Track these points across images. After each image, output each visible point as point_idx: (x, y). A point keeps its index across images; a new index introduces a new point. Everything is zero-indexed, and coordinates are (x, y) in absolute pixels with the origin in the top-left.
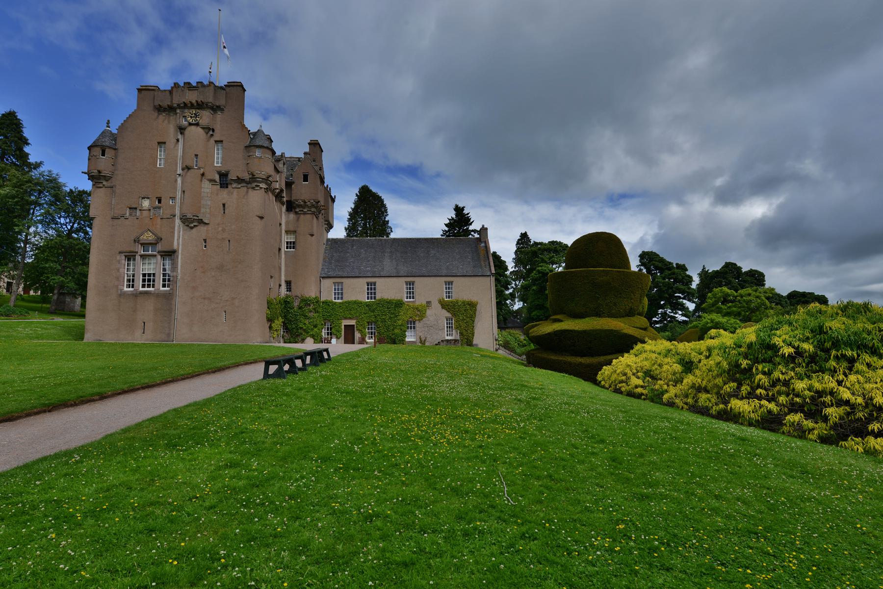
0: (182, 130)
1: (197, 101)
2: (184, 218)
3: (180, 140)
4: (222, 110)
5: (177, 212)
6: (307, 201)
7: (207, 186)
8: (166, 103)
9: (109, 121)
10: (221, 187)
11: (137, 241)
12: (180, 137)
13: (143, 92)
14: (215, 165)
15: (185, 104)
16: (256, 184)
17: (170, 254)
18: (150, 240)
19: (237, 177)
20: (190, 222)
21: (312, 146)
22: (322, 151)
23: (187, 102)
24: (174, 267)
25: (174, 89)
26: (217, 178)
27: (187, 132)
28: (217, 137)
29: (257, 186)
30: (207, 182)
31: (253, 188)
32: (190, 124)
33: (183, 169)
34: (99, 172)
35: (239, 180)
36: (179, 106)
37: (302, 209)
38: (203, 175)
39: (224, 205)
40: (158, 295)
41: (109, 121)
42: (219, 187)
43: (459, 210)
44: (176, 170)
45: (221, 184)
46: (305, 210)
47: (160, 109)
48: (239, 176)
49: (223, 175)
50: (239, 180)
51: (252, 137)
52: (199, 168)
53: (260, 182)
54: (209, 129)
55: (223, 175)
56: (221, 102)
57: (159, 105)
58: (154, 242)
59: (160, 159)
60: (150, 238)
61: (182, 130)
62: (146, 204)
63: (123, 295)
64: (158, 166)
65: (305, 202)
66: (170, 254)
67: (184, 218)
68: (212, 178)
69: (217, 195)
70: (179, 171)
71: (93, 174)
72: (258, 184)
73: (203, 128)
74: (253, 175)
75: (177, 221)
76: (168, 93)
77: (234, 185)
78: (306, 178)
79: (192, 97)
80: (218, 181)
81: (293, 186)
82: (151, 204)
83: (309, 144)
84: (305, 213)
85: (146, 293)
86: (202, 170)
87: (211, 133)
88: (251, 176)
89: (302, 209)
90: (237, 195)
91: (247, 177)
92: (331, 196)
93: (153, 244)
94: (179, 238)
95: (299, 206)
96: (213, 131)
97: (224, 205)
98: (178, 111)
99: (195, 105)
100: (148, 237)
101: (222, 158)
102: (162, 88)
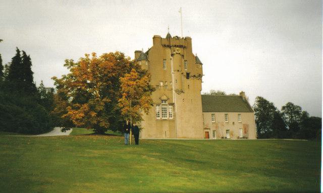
5: (173, 88)
8: (167, 43)
17: (173, 104)
20: (180, 92)
24: (174, 109)
33: (174, 71)
36: (173, 46)
40: (170, 121)
47: (165, 46)
63: (157, 120)
66: (173, 104)
70: (172, 71)
75: (174, 92)
77: (192, 78)
79: (178, 43)
85: (165, 120)
94: (175, 98)
98: (172, 48)
100: (164, 98)
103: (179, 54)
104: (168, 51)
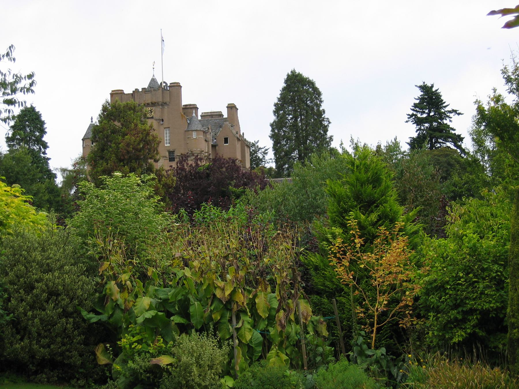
4: (168, 105)
9: (92, 117)
10: (170, 161)
13: (114, 95)
14: (166, 145)
21: (230, 109)
22: (237, 109)
25: (136, 94)
26: (167, 154)
41: (92, 117)
43: (426, 89)
45: (169, 158)
54: (160, 120)
56: (167, 100)
68: (164, 155)
73: (156, 120)
76: (131, 96)
78: (226, 140)
79: (148, 99)
80: (168, 157)
81: (217, 148)
83: (227, 107)
96: (163, 120)
99: (150, 104)
101: (169, 140)
102: (126, 92)
103: (152, 118)
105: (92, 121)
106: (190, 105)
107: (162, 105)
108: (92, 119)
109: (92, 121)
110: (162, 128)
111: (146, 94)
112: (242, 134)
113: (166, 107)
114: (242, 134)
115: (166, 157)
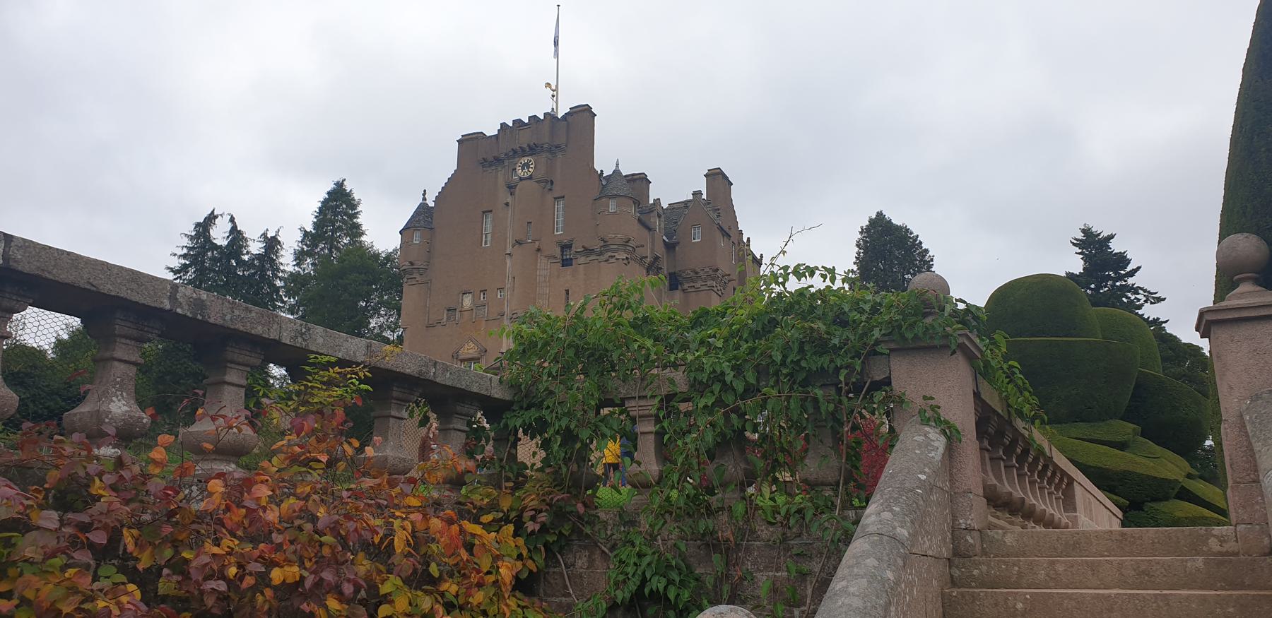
0: (511, 188)
1: (529, 145)
2: (514, 316)
3: (510, 203)
6: (698, 270)
7: (544, 267)
9: (425, 191)
11: (455, 356)
12: (509, 200)
15: (515, 152)
16: (610, 254)
18: (472, 354)
19: (583, 247)
23: (516, 147)
26: (558, 250)
27: (517, 191)
28: (557, 191)
29: (612, 257)
30: (544, 260)
31: (606, 261)
32: (521, 179)
34: (412, 264)
35: (587, 251)
37: (692, 284)
38: (539, 250)
39: (567, 291)
41: (425, 191)
42: (560, 265)
44: (505, 249)
45: (563, 260)
46: (698, 285)
47: (485, 163)
48: (586, 245)
49: (565, 247)
50: (587, 251)
51: (604, 183)
52: (534, 241)
53: (616, 250)
54: (546, 181)
55: (565, 247)
57: (484, 159)
58: (476, 356)
59: (486, 235)
60: (471, 351)
61: (511, 188)
62: (467, 301)
64: (483, 245)
65: (697, 273)
67: (514, 316)
69: (558, 277)
71: (404, 268)
72: (613, 254)
74: (605, 242)
77: (582, 260)
79: (524, 139)
81: (677, 248)
82: (473, 300)
84: (698, 291)
86: (537, 243)
87: (549, 186)
88: (602, 243)
89: (692, 284)
90: (585, 275)
91: (597, 245)
92: (754, 257)
93: (476, 360)
95: (689, 279)
96: (552, 183)
97: (567, 291)
98: (506, 163)
100: (470, 350)
101: (564, 221)
103: (530, 178)
104: (501, 176)
105: (424, 199)
106: (633, 175)
107: (550, 151)
108: (424, 194)
109: (424, 199)
110: (550, 197)
111: (521, 132)
112: (745, 240)
113: (559, 155)
114: (745, 240)
115: (554, 257)
